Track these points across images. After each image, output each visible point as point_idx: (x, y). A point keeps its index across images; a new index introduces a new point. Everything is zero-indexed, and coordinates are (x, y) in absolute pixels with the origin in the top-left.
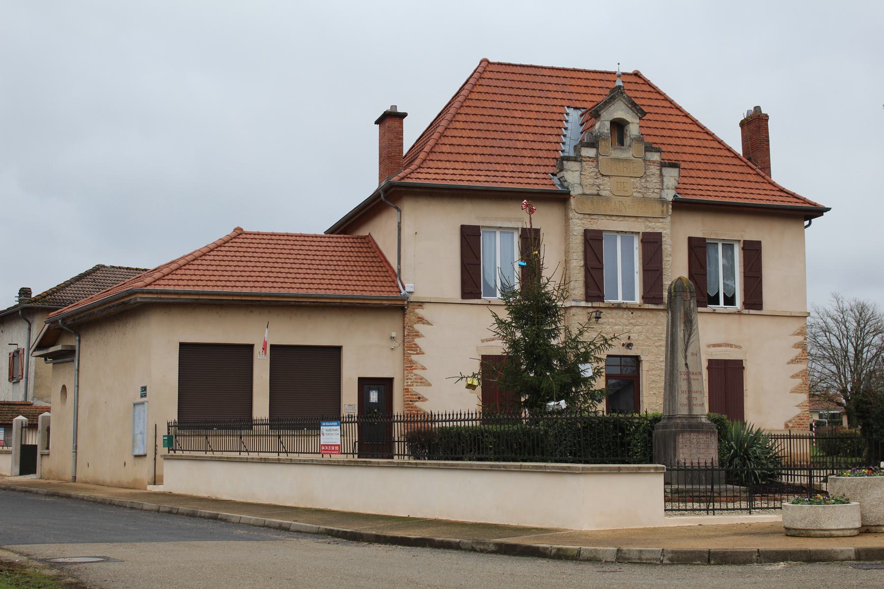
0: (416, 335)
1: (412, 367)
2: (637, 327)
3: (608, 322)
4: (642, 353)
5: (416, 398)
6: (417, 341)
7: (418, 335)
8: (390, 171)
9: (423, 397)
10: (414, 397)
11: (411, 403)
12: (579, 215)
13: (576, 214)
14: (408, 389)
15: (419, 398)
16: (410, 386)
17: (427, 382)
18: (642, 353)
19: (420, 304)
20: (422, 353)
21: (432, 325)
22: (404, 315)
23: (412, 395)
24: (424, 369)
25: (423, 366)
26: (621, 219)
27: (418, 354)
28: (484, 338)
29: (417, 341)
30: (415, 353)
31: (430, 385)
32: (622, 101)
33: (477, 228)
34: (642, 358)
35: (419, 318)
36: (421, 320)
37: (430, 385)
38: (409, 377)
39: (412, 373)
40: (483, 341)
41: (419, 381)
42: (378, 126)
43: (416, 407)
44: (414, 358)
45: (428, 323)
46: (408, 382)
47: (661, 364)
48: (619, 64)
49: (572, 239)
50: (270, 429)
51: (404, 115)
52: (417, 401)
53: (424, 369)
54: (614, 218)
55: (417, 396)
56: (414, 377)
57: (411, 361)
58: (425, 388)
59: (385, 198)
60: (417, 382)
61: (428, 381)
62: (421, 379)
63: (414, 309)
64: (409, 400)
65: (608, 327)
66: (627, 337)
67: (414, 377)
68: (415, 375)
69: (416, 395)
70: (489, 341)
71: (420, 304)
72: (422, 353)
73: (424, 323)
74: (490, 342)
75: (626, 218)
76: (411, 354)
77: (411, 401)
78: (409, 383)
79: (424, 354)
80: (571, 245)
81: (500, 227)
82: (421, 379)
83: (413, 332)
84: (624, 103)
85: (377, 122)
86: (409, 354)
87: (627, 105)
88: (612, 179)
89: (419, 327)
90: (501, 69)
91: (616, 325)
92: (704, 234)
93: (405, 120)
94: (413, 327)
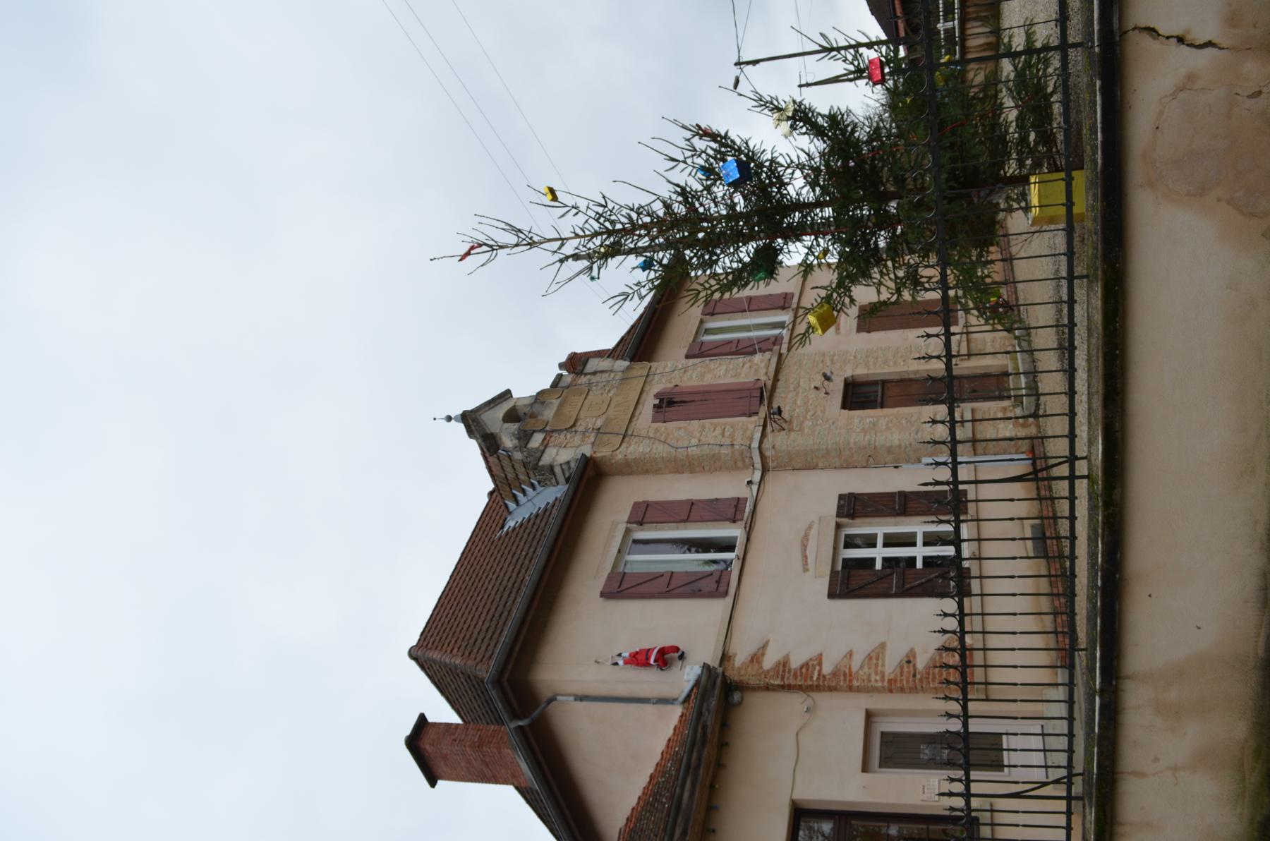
0: (784, 665)
1: (845, 674)
2: (802, 383)
3: (789, 410)
4: (841, 376)
5: (908, 667)
6: (795, 663)
7: (784, 663)
8: (502, 745)
9: (907, 656)
10: (906, 669)
11: (918, 676)
12: (622, 447)
13: (621, 449)
14: (890, 681)
15: (909, 662)
16: (883, 677)
17: (877, 650)
18: (841, 376)
19: (725, 657)
20: (819, 659)
21: (767, 642)
22: (742, 687)
23: (901, 675)
24: (850, 654)
25: (845, 656)
26: (640, 407)
27: (820, 664)
28: (800, 567)
29: (795, 663)
30: (817, 668)
31: (883, 646)
32: (482, 414)
33: (611, 576)
34: (849, 374)
35: (752, 661)
36: (756, 658)
37: (883, 646)
38: (865, 677)
39: (857, 672)
40: (806, 570)
41: (874, 661)
42: (440, 782)
43: (927, 667)
44: (827, 669)
45: (764, 647)
46: (876, 680)
47: (859, 357)
48: (435, 419)
49: (656, 454)
50: (999, 766)
51: (422, 718)
52: (914, 665)
53: (850, 654)
54: (637, 413)
55: (906, 665)
56: (866, 670)
57: (834, 674)
58: (888, 652)
59: (525, 717)
60: (877, 665)
61: (876, 648)
62: (870, 659)
63: (733, 668)
64: (911, 679)
65: (797, 410)
66: (816, 391)
67: (866, 670)
68: (861, 667)
69: (902, 668)
70: (806, 561)
71: (725, 657)
72: (819, 659)
73: (763, 654)
74: (809, 560)
75: (641, 401)
76: (819, 674)
77: (914, 676)
78: (878, 678)
79: (821, 654)
80: (664, 455)
81: (619, 551)
82: (870, 659)
83: (778, 670)
84: (486, 411)
85: (433, 783)
86: (818, 679)
87: (490, 409)
88: (582, 415)
89: (769, 662)
90: (429, 625)
91: (795, 402)
92: (685, 347)
93: (430, 719)
94: (768, 671)
